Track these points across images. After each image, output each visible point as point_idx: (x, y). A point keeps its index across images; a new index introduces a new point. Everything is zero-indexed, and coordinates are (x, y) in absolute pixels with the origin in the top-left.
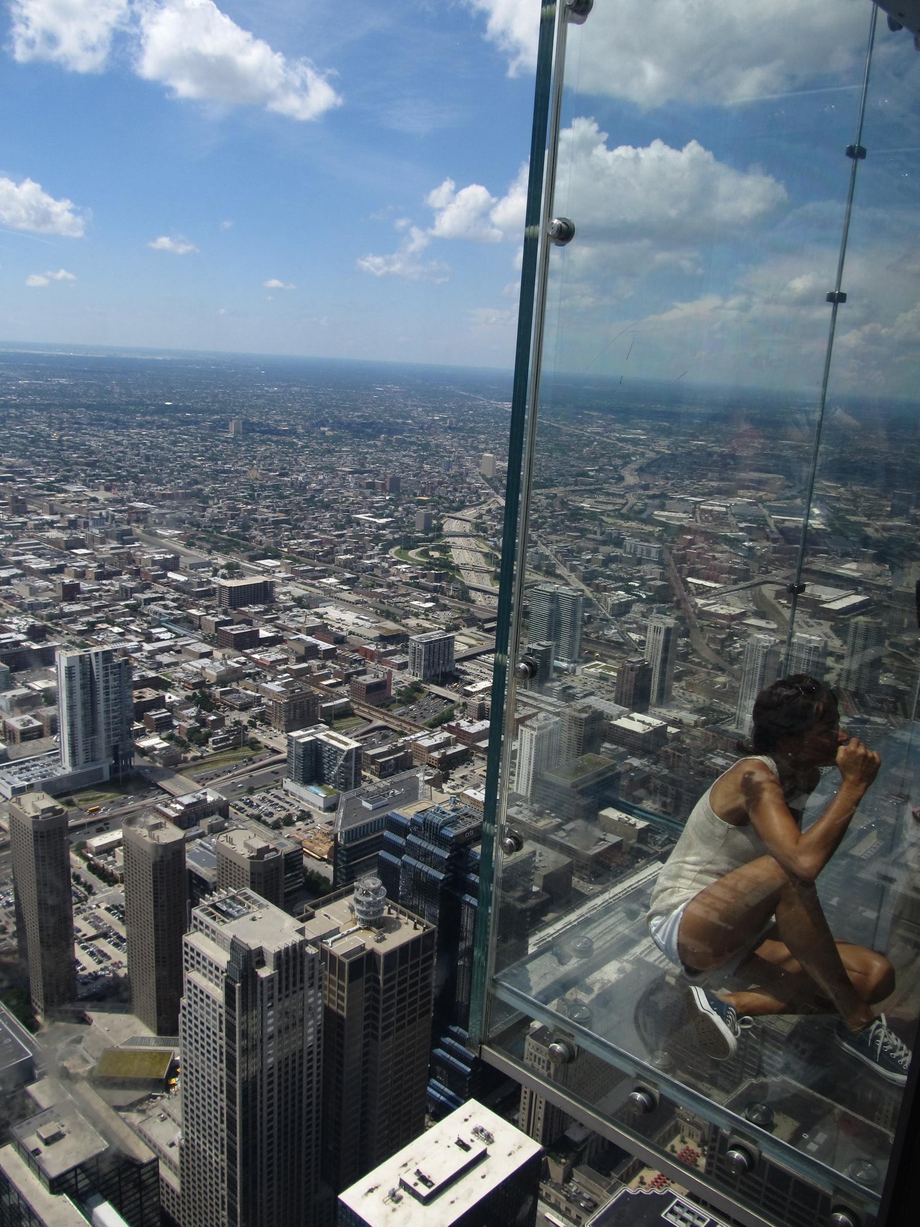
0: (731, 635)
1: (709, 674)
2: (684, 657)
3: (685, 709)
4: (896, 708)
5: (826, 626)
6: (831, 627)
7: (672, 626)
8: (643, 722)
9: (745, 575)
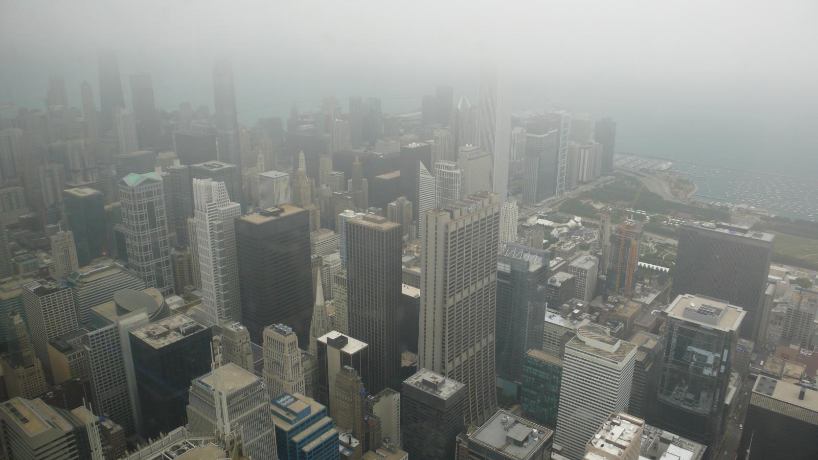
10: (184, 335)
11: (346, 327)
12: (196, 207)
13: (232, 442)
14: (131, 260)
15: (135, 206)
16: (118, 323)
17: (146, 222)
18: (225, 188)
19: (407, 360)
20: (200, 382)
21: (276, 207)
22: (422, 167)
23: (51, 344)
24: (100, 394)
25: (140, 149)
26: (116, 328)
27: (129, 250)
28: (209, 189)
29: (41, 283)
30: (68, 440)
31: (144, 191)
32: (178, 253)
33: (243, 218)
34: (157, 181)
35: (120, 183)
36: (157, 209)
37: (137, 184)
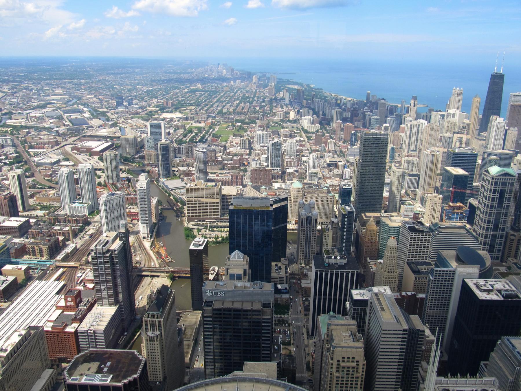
0: (54, 172)
1: (46, 191)
2: (33, 187)
3: (37, 209)
4: (129, 186)
5: (96, 158)
6: (99, 159)
7: (20, 173)
8: (17, 221)
9: (57, 143)
14: (475, 226)
16: (456, 268)
17: (495, 203)
23: (407, 263)
24: (429, 310)
25: (503, 149)
26: (454, 271)
27: (476, 220)
29: (414, 223)
31: (501, 181)
32: (512, 233)
35: (485, 171)
36: (507, 196)
37: (498, 174)
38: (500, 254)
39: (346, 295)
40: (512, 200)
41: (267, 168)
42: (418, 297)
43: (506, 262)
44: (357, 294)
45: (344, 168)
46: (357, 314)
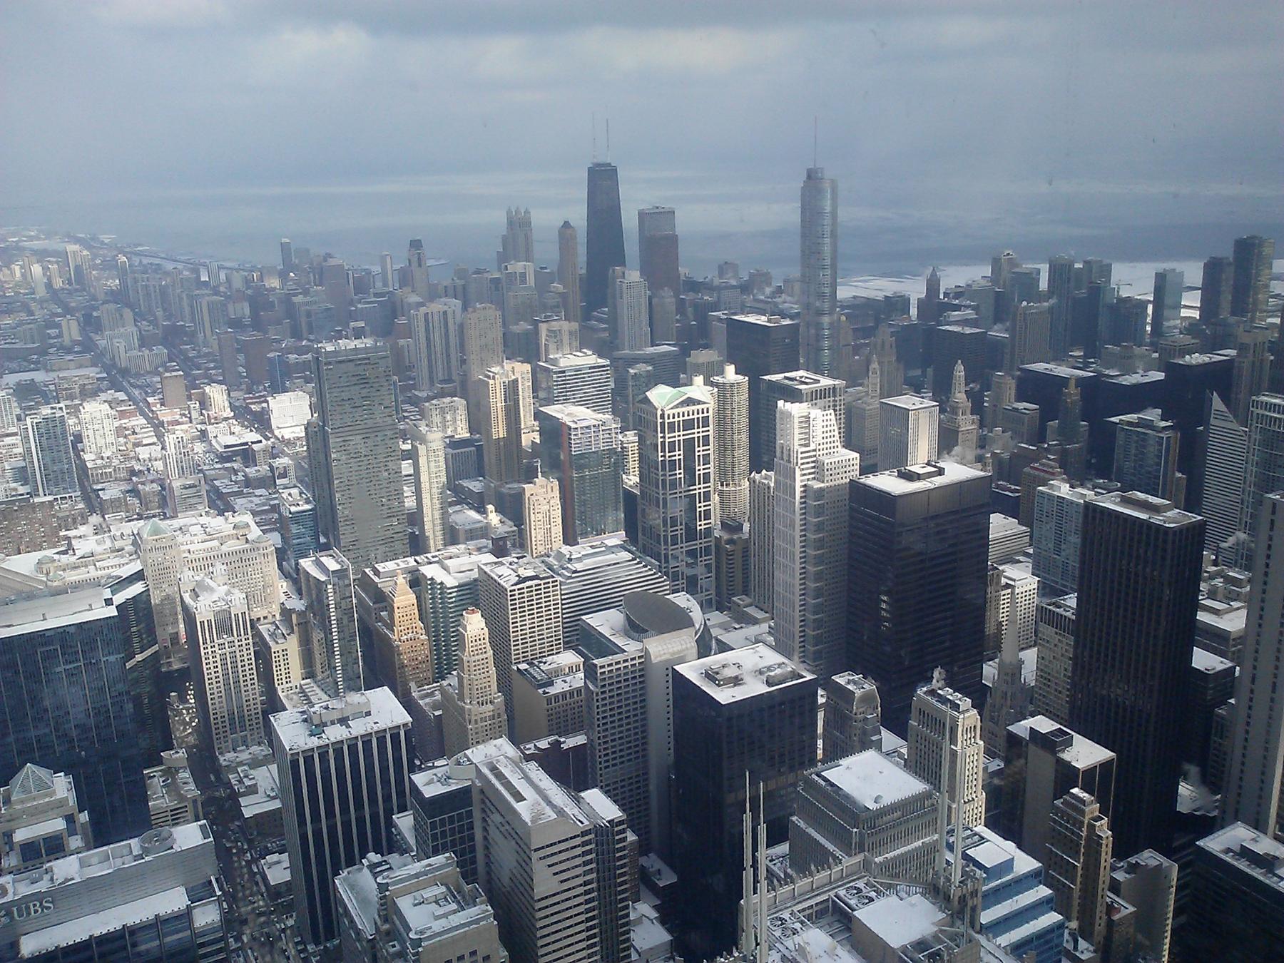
10: (769, 684)
11: (1065, 712)
12: (778, 454)
13: (963, 900)
15: (663, 443)
18: (834, 422)
19: (1187, 794)
20: (819, 775)
21: (928, 464)
22: (1217, 403)
24: (603, 771)
28: (806, 420)
30: (584, 844)
32: (726, 536)
33: (864, 480)
34: (699, 402)
36: (699, 451)
38: (713, 591)
39: (387, 798)
40: (712, 457)
41: (37, 500)
42: (565, 746)
43: (729, 609)
44: (429, 783)
45: (274, 457)
46: (443, 832)
